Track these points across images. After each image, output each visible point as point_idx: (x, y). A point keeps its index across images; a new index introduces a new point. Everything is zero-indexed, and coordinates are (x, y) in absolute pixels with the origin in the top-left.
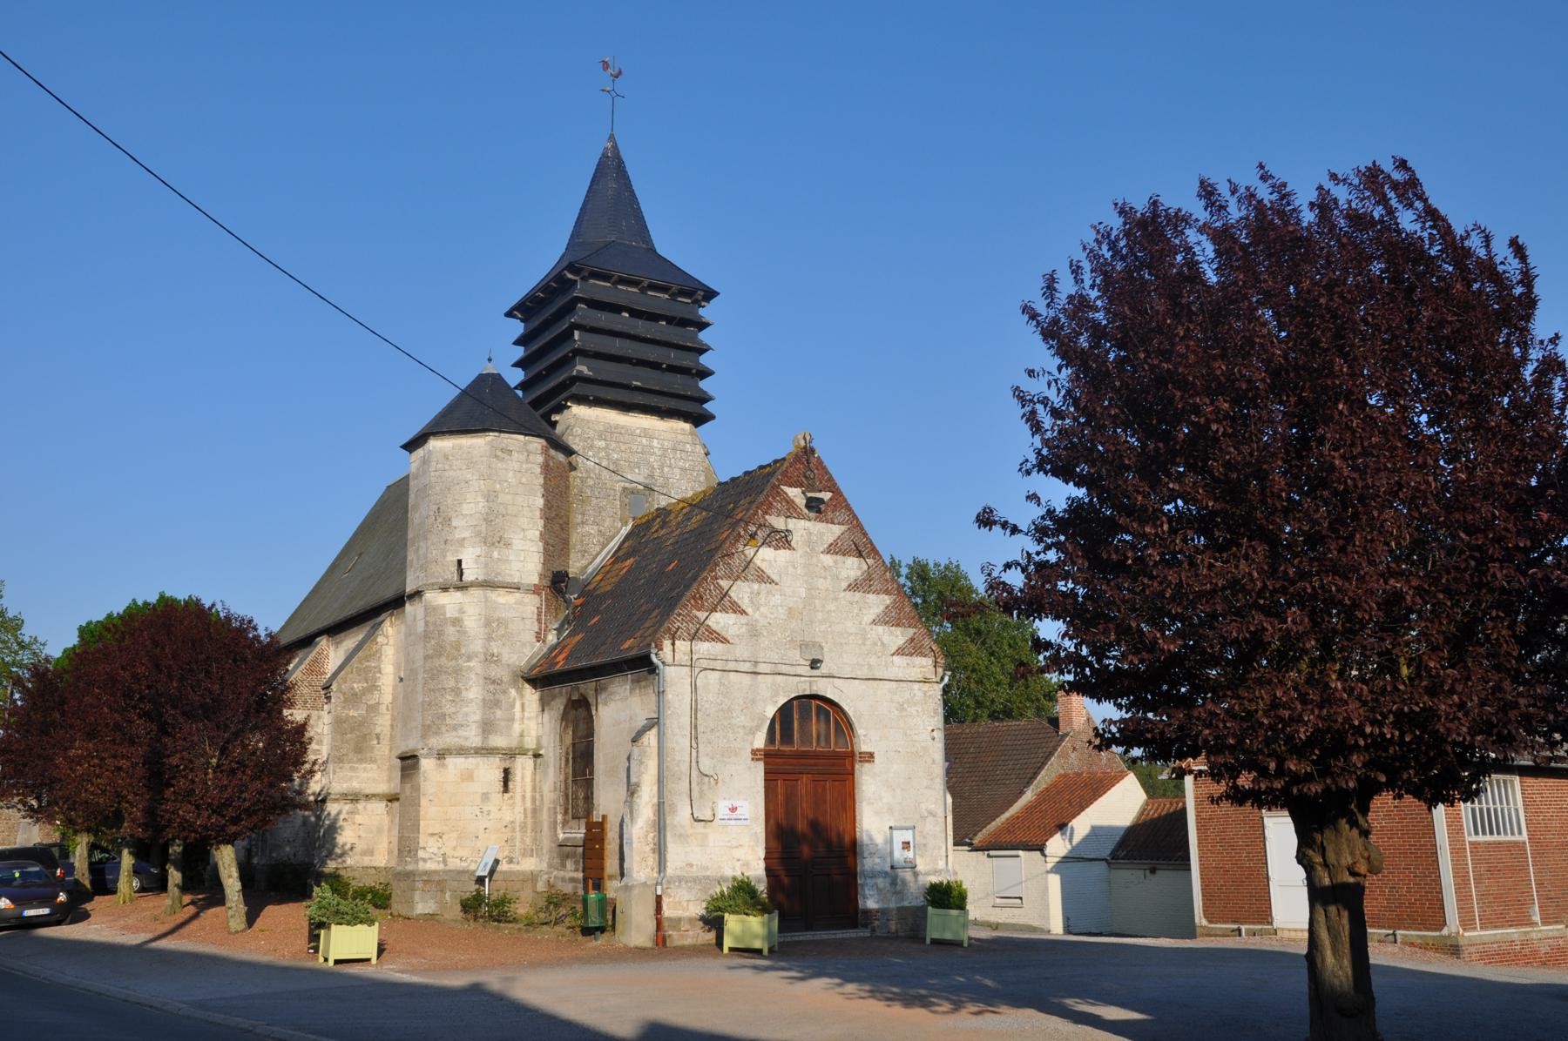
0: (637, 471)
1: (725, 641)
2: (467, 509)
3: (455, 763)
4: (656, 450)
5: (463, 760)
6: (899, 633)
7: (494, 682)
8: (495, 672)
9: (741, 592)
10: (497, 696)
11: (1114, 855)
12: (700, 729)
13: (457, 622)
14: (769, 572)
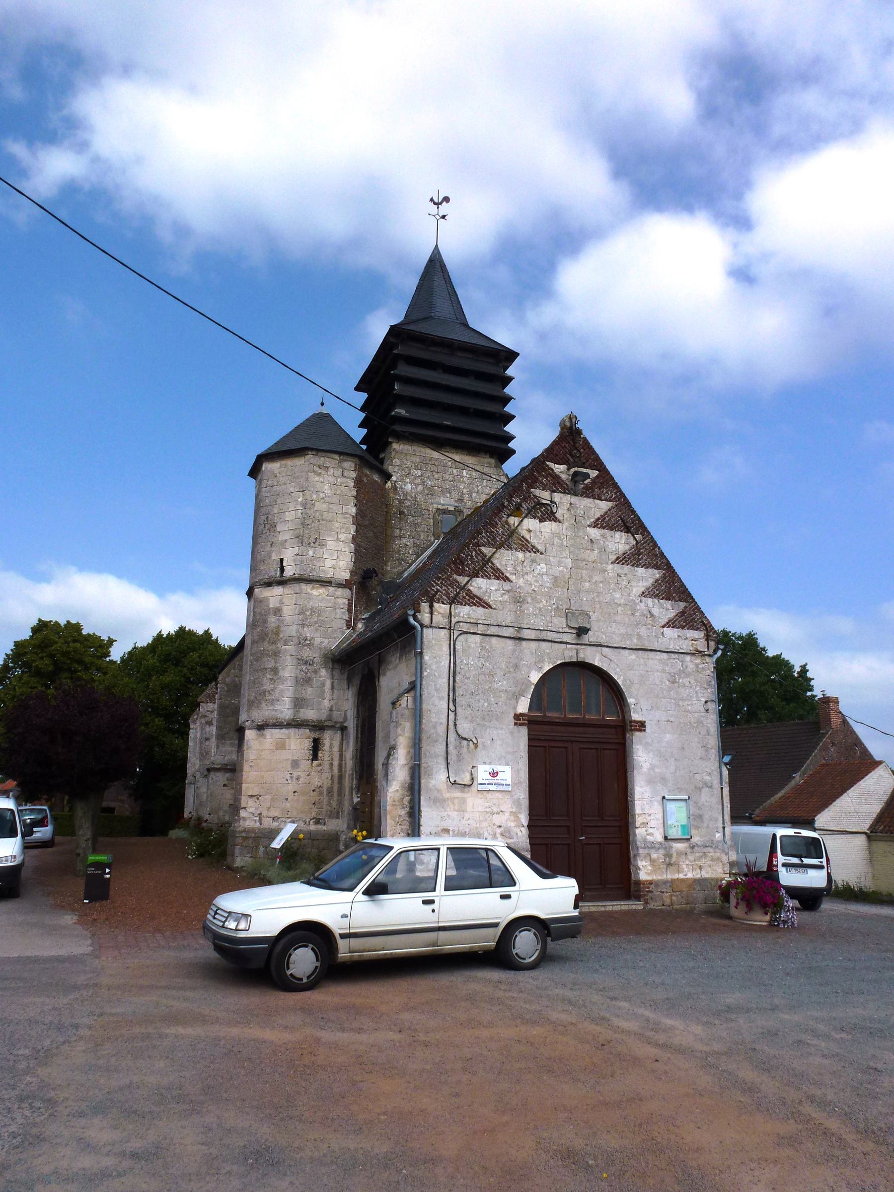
0: (448, 495)
1: (487, 606)
2: (289, 516)
3: (273, 734)
5: (278, 730)
6: (670, 607)
7: (306, 663)
8: (307, 653)
9: (505, 559)
10: (309, 675)
11: (873, 828)
12: (459, 692)
13: (278, 611)
14: (534, 541)
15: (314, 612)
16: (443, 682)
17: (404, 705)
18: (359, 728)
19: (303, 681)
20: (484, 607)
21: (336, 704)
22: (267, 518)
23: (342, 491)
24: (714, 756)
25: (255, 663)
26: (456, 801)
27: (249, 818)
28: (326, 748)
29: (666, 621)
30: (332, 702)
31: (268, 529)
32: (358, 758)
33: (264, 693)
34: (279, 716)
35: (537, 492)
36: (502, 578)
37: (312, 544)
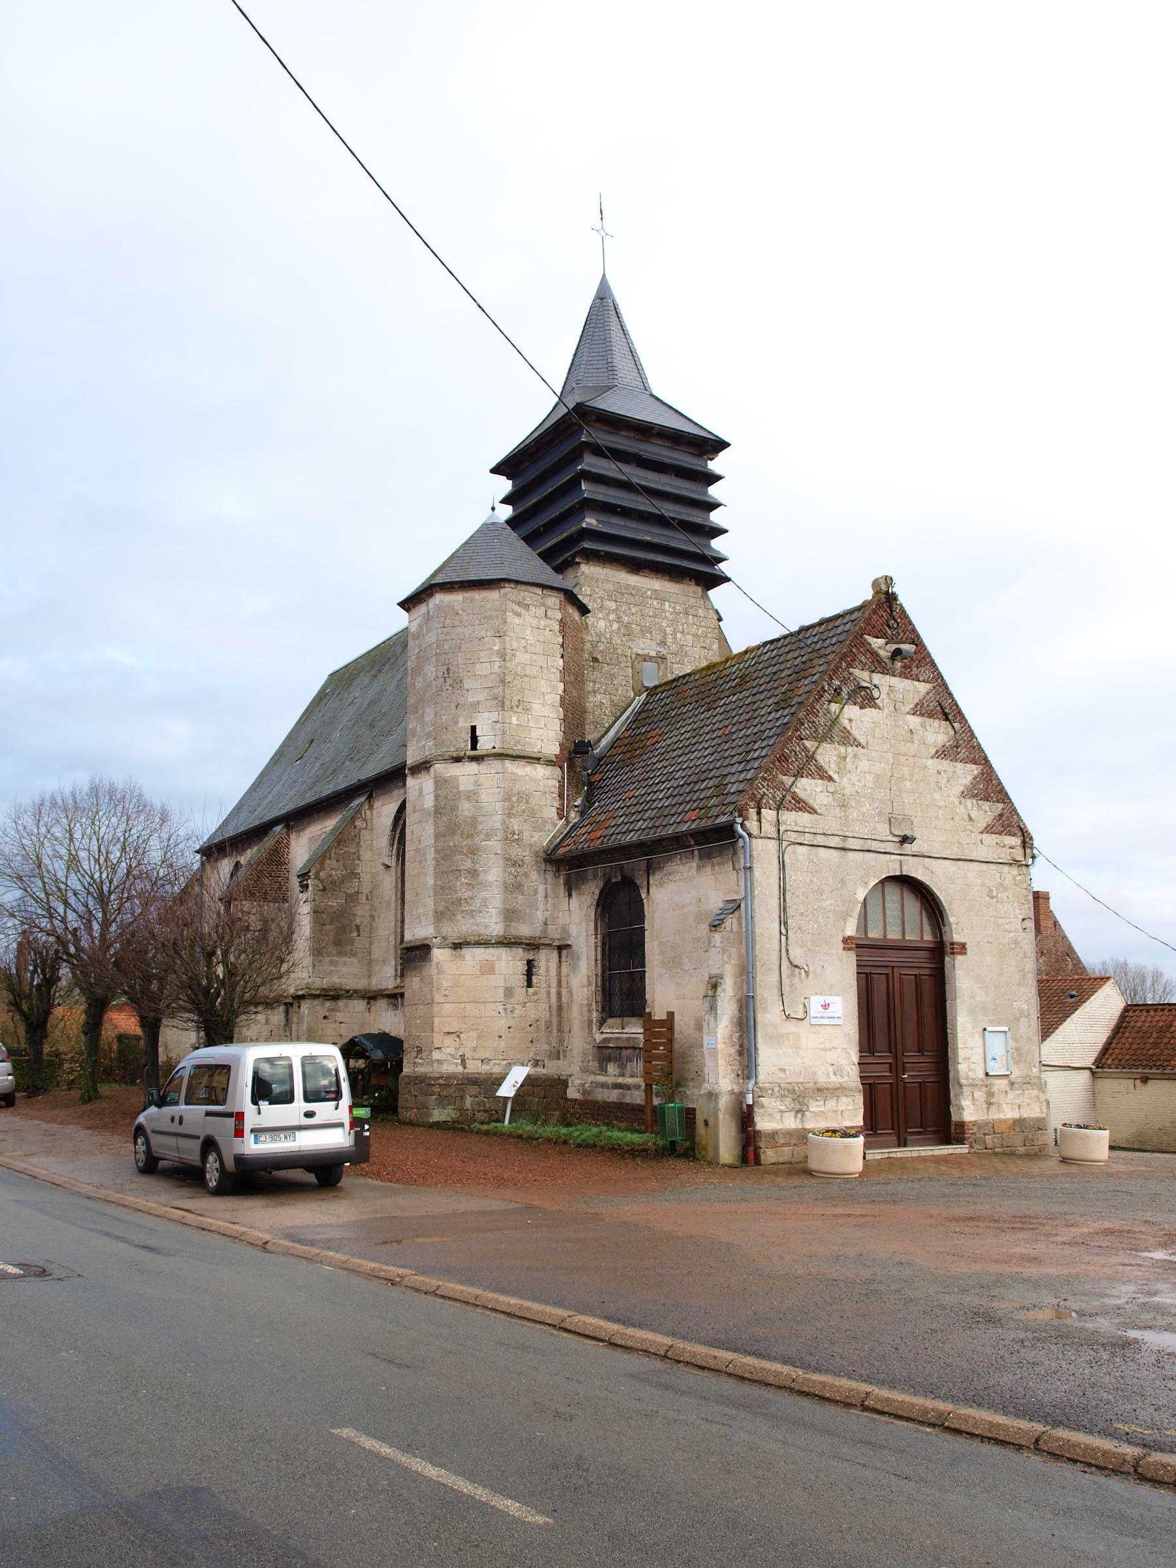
0: (648, 635)
1: (812, 811)
2: (481, 669)
3: (473, 957)
4: (668, 615)
5: (483, 950)
6: (987, 808)
7: (515, 864)
8: (515, 852)
9: (827, 755)
10: (519, 878)
11: (1100, 1062)
12: (790, 912)
13: (472, 796)
14: (855, 733)
15: (522, 797)
16: (774, 902)
17: (728, 929)
18: (599, 948)
19: (513, 888)
20: (810, 813)
21: (551, 915)
22: (448, 669)
23: (546, 637)
24: (1030, 982)
25: (442, 862)
26: (791, 1037)
27: (446, 1060)
28: (542, 971)
29: (985, 825)
30: (547, 914)
31: (450, 685)
32: (599, 984)
33: (459, 902)
34: (482, 932)
35: (856, 672)
36: (826, 777)
37: (515, 708)
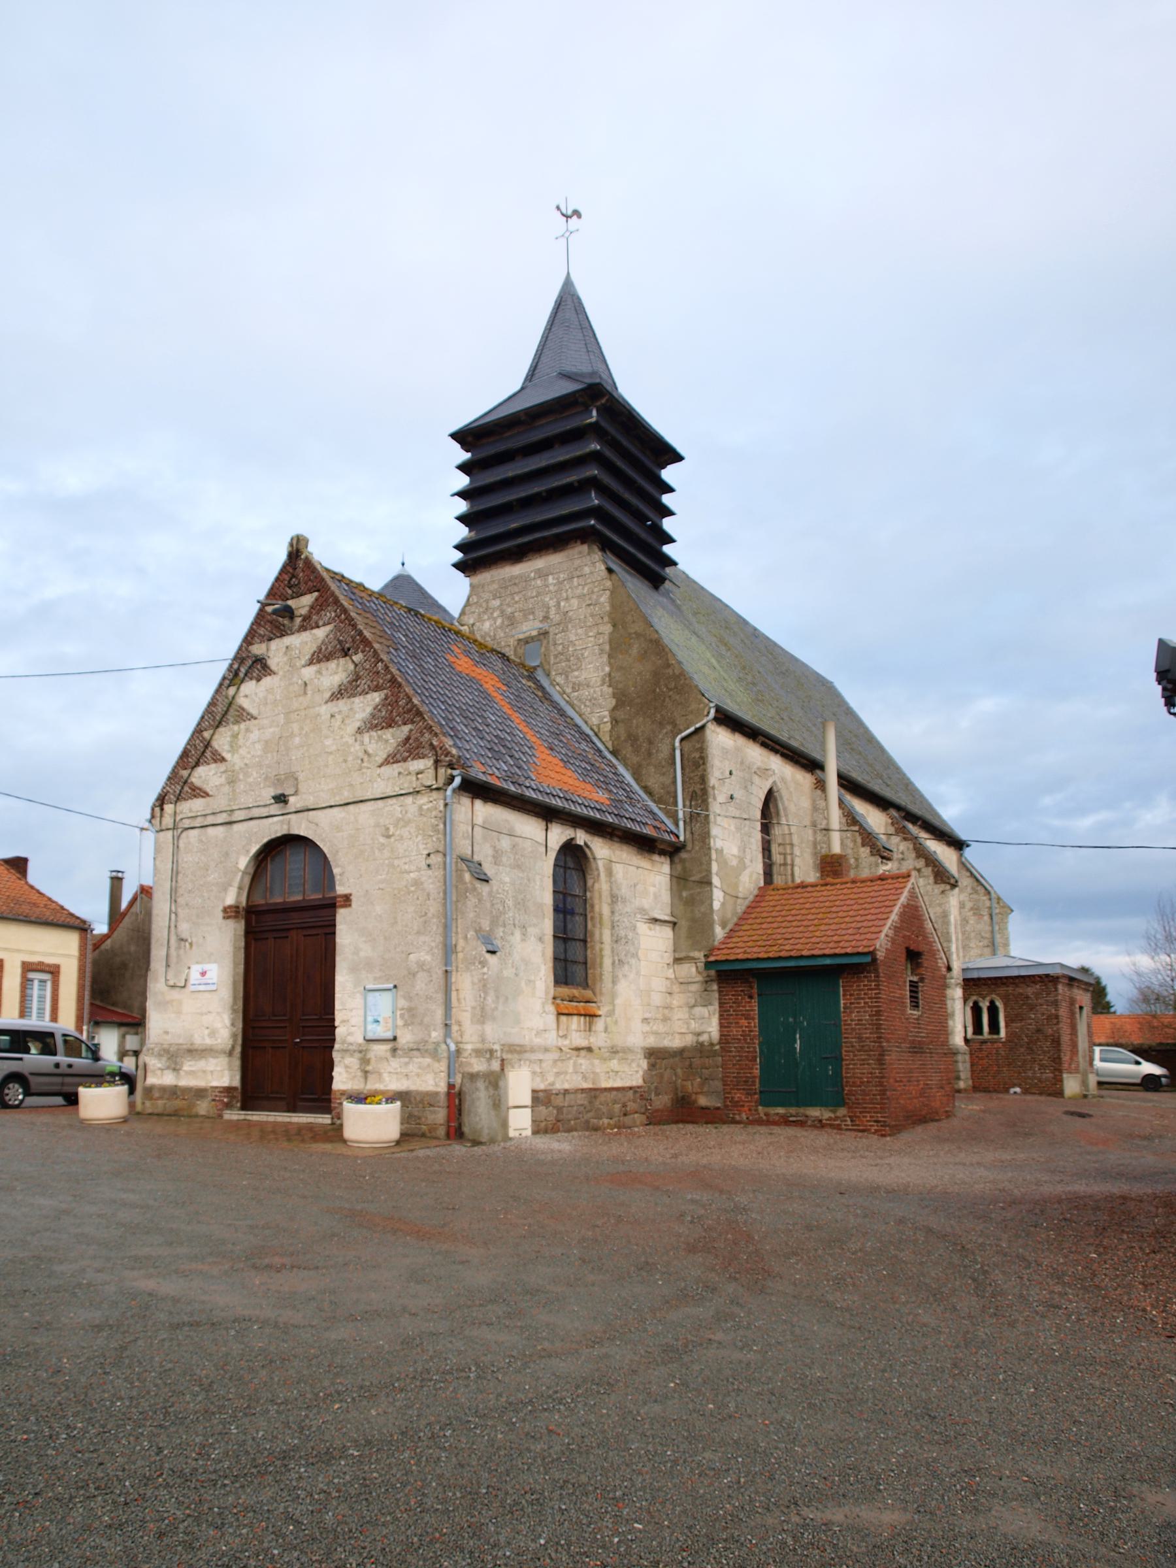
20: (203, 797)
24: (435, 928)
29: (385, 756)
